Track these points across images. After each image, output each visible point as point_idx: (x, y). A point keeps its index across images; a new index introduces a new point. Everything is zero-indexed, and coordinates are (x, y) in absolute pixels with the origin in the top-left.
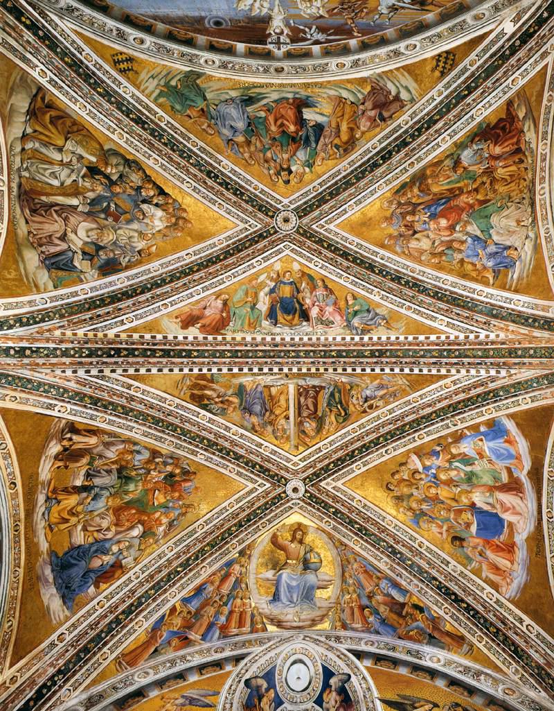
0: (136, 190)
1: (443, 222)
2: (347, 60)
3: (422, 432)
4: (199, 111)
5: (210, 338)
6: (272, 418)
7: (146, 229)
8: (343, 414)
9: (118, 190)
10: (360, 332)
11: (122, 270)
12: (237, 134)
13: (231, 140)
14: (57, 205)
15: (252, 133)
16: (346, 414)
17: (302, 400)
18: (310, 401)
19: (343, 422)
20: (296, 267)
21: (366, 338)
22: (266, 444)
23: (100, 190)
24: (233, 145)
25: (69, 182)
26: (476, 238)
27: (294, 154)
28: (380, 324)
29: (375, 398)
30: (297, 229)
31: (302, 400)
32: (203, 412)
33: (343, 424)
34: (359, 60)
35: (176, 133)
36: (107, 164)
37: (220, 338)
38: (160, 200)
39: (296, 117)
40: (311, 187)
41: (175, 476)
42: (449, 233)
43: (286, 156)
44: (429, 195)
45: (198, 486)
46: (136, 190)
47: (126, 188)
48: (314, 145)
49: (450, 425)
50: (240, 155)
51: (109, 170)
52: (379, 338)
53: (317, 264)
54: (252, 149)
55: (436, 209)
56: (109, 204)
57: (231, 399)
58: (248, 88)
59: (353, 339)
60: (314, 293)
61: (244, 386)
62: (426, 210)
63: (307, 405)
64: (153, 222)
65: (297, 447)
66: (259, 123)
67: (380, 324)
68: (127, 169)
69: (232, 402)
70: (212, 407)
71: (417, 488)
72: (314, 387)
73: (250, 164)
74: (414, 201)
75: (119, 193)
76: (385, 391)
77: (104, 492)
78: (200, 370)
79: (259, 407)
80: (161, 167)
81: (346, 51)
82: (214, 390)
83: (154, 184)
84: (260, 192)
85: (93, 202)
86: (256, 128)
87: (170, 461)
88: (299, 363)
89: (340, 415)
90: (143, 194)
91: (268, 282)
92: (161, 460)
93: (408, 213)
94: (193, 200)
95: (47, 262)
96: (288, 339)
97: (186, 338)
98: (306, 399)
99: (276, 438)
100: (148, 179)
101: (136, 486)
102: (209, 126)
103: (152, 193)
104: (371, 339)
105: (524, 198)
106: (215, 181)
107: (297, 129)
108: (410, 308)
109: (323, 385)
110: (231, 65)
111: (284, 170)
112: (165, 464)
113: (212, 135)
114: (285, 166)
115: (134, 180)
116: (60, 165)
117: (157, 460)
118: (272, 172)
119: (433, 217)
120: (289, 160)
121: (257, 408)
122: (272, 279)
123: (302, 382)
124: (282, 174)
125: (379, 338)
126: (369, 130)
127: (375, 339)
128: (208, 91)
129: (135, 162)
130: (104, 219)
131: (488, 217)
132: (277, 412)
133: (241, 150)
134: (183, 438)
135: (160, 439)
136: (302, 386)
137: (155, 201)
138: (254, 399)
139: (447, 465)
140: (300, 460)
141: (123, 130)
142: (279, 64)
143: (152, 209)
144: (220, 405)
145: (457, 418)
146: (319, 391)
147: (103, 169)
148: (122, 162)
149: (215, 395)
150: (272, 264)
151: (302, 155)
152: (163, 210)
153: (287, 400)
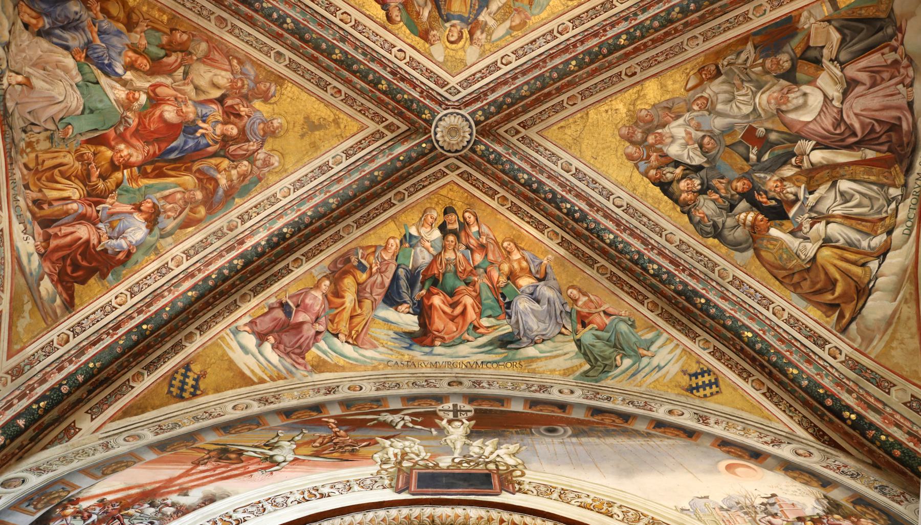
0: (709, 188)
1: (170, 113)
2: (343, 393)
4: (589, 323)
7: (700, 120)
9: (739, 185)
11: (755, 34)
12: (531, 289)
13: (539, 280)
14: (849, 147)
15: (504, 291)
20: (438, 51)
23: (771, 182)
24: (537, 272)
25: (822, 190)
26: (108, 71)
27: (435, 258)
30: (434, 117)
34: (326, 394)
35: (631, 287)
36: (753, 226)
38: (670, 173)
39: (430, 318)
40: (408, 201)
42: (159, 90)
43: (450, 255)
44: (199, 170)
46: (709, 188)
47: (726, 189)
48: (401, 272)
50: (526, 254)
51: (751, 217)
53: (401, 55)
54: (506, 267)
55: (186, 143)
56: (759, 159)
58: (506, 360)
62: (203, 142)
64: (688, 133)
66: (491, 308)
68: (720, 221)
73: (512, 241)
74: (226, 163)
75: (739, 180)
80: (662, 229)
81: (346, 404)
83: (676, 201)
84: (496, 192)
85: (784, 160)
86: (498, 301)
90: (697, 182)
91: (491, 22)
93: (235, 140)
94: (613, 177)
95: (890, 31)
100: (687, 208)
102: (575, 301)
103: (683, 185)
105: (25, 131)
106: (573, 205)
107: (429, 299)
110: (533, 388)
111: (454, 232)
113: (573, 287)
114: (451, 238)
115: (712, 205)
116: (833, 216)
118: (475, 229)
119: (190, 128)
120: (444, 248)
122: (484, 27)
124: (456, 226)
126: (306, 292)
128: (572, 354)
129: (704, 234)
130: (772, 130)
131: (88, 110)
133: (524, 264)
137: (679, 171)
141: (718, 283)
142: (456, 389)
143: (686, 156)
147: (760, 217)
148: (726, 232)
150: (482, 56)
151: (422, 257)
152: (665, 156)
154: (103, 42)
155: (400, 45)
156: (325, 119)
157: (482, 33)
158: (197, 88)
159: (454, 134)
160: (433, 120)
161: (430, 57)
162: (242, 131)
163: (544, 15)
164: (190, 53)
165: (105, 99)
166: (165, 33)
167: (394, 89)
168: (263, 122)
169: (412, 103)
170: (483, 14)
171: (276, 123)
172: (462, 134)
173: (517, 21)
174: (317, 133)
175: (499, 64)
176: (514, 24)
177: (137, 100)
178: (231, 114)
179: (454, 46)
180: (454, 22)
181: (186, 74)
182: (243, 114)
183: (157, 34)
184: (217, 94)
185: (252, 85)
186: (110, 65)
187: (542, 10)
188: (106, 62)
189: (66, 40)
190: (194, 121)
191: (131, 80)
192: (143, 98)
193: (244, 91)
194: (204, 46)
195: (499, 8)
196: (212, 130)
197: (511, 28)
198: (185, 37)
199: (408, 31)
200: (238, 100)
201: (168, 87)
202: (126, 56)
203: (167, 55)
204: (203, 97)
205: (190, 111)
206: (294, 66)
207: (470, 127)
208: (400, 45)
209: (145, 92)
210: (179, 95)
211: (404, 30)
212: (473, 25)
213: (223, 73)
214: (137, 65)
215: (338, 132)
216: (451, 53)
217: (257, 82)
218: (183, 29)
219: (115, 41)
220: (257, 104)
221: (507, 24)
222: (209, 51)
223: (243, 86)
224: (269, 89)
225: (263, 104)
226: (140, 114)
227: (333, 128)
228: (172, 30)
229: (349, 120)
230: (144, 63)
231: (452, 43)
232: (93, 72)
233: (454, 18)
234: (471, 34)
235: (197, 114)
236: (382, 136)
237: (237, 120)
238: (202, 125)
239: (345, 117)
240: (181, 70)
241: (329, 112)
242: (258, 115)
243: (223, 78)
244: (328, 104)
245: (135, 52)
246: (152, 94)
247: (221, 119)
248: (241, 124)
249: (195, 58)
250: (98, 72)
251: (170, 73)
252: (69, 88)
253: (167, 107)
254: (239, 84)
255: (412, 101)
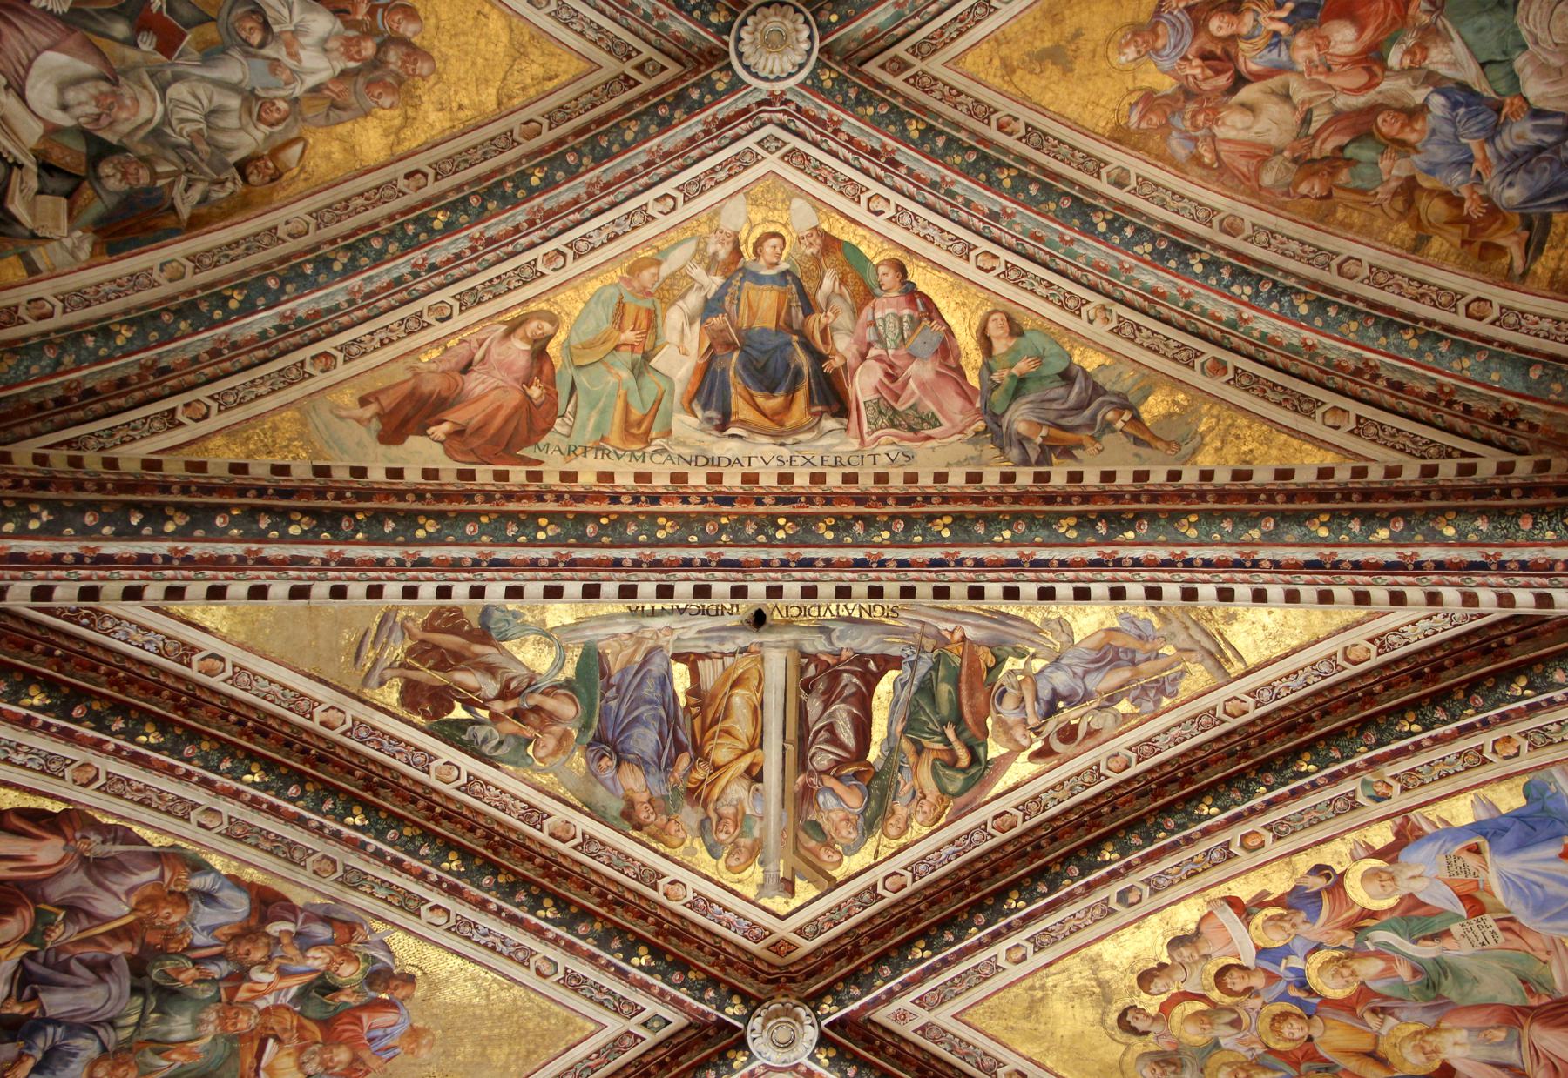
3: (1257, 823)
5: (484, 475)
6: (700, 774)
8: (964, 760)
10: (1033, 456)
16: (975, 759)
17: (814, 706)
18: (842, 715)
19: (965, 789)
20: (801, 217)
21: (1058, 479)
22: (673, 871)
28: (1108, 426)
29: (1087, 696)
31: (814, 706)
32: (446, 752)
33: (962, 800)
37: (518, 475)
41: (336, 989)
45: (419, 1024)
49: (1361, 799)
52: (1108, 476)
57: (550, 704)
59: (1008, 478)
60: (866, 313)
61: (601, 657)
63: (830, 728)
65: (788, 887)
67: (1108, 426)
69: (553, 718)
70: (482, 732)
71: (1236, 1024)
72: (861, 659)
76: (1124, 674)
77: (80, 1042)
78: (444, 593)
79: (653, 736)
82: (491, 670)
87: (321, 931)
88: (808, 564)
89: (952, 764)
91: (698, 272)
92: (289, 926)
96: (768, 481)
97: (395, 473)
98: (827, 704)
99: (713, 852)
101: (197, 1023)
104: (1075, 477)
108: (1218, 367)
109: (894, 651)
112: (304, 941)
117: (274, 928)
121: (645, 740)
122: (711, 264)
123: (816, 644)
125: (1108, 476)
127: (1092, 479)
132: (721, 754)
134: (374, 844)
135: (288, 852)
136: (813, 657)
138: (637, 702)
139: (1348, 939)
140: (800, 932)
144: (511, 726)
145: (1389, 771)
146: (878, 676)
149: (491, 688)
153: (758, 710)
154: (1467, 145)
155: (880, 224)
156: (1032, 72)
157: (715, 254)
158: (1286, 97)
159: (775, 37)
160: (815, 69)
161: (817, 203)
162: (1199, 26)
163: (593, 286)
164: (1295, 161)
165: (1470, 37)
166: (1343, 188)
167: (894, 124)
168: (1157, 52)
169: (857, 98)
170: (714, 288)
171: (1131, 52)
172: (758, 35)
173: (646, 275)
174: (1048, 44)
175: (680, 196)
176: (653, 270)
177: (1409, 51)
178: (1219, 58)
179: (772, 228)
180: (772, 272)
181: (1306, 121)
182: (1197, 62)
183: (1358, 183)
184: (1247, 93)
185: (1176, 121)
186: (1455, 105)
187: (596, 295)
188: (1462, 111)
189: (1536, 129)
190: (1296, 31)
191: (1415, 88)
192: (1394, 58)
193: (1191, 107)
194: (1268, 179)
195: (682, 297)
196: (1261, 19)
197: (659, 263)
198: (1304, 188)
199: (863, 248)
200: (1205, 86)
201: (1345, 90)
202: (1422, 132)
203: (1341, 149)
204: (1275, 82)
205: (1303, 51)
206: (1091, 166)
207: (740, 55)
208: (880, 224)
209: (1391, 69)
210: (1322, 78)
211: (872, 251)
212: (733, 268)
213: (1232, 134)
214: (1403, 117)
215: (1004, 51)
216: (775, 215)
217: (1166, 127)
218: (1307, 201)
219: (1440, 154)
220: (1167, 85)
221: (665, 270)
222: (1257, 172)
223: (1194, 117)
224: (1142, 118)
225: (1155, 86)
226: (1405, 23)
227: (1016, 55)
228: (1329, 196)
229: (982, 76)
230: (1387, 125)
231: (775, 235)
232: (1490, 83)
233: (772, 279)
234: (737, 252)
235: (1288, 47)
236: (915, 50)
237: (1210, 46)
238: (1281, 27)
239: (990, 79)
240: (1314, 127)
241: (1023, 86)
242: (1166, 65)
243: (1233, 126)
244: (1025, 101)
245: (1403, 143)
246: (1376, 68)
247: (1242, 45)
248: (1202, 40)
249: (1286, 154)
250: (1481, 86)
251: (1338, 116)
252: (1542, 35)
253: (1348, 49)
254: (1201, 118)
255: (858, 102)
